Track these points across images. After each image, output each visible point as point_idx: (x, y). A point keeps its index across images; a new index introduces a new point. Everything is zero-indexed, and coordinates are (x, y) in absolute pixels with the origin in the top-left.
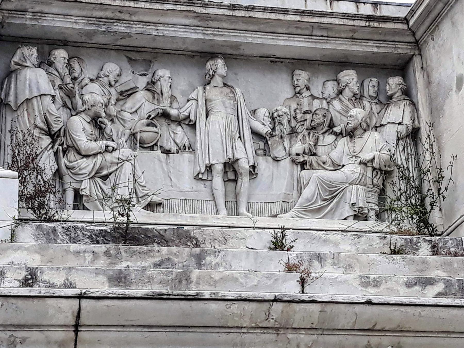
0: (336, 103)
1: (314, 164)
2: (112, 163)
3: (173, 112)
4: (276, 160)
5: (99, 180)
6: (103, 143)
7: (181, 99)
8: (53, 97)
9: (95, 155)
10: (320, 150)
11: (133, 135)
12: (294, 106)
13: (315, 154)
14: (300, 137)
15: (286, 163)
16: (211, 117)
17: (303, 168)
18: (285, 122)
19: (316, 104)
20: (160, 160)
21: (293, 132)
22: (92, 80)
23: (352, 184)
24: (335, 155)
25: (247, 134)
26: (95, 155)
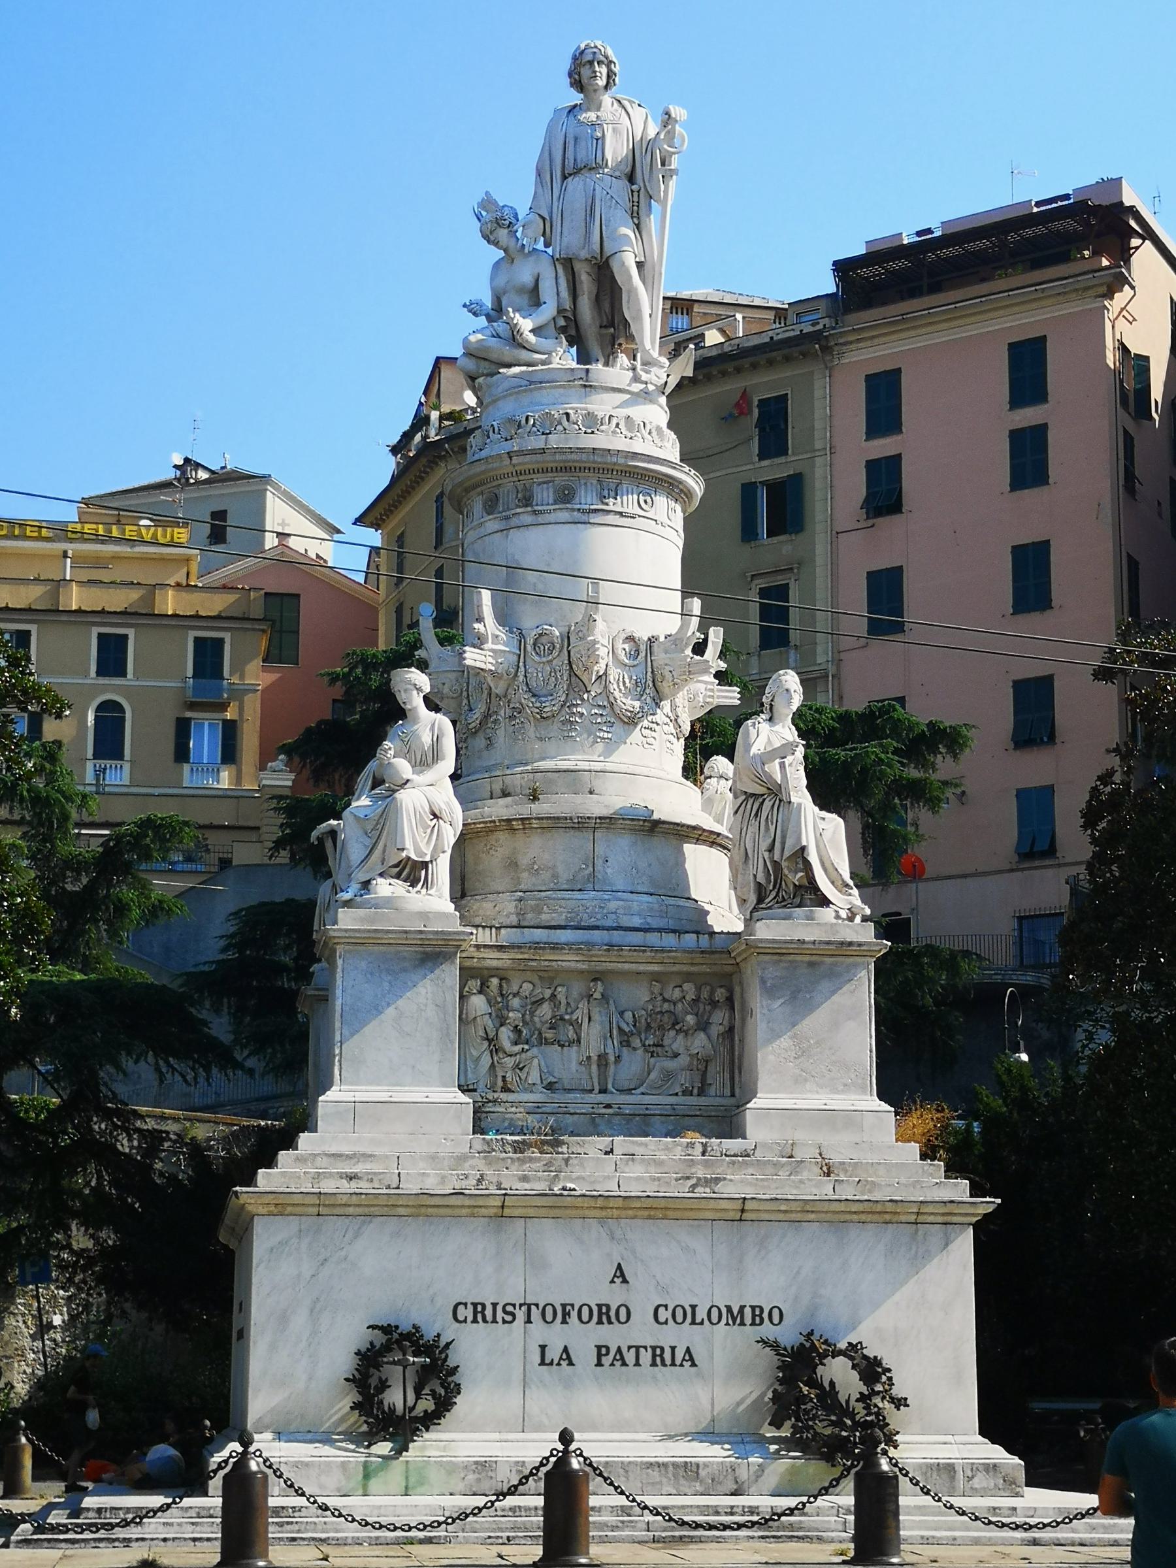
0: (680, 1005)
1: (660, 1054)
2: (526, 1060)
3: (567, 1017)
4: (635, 1049)
5: (518, 1071)
6: (521, 1046)
7: (573, 1005)
8: (490, 1014)
9: (516, 1055)
10: (666, 1042)
11: (540, 1033)
12: (650, 1007)
13: (662, 1046)
14: (652, 1031)
15: (640, 1052)
16: (591, 1023)
17: (652, 1056)
18: (643, 1021)
19: (666, 1006)
20: (556, 1051)
21: (648, 1027)
22: (514, 996)
23: (682, 1070)
24: (674, 1047)
25: (615, 1032)
26: (516, 1055)
